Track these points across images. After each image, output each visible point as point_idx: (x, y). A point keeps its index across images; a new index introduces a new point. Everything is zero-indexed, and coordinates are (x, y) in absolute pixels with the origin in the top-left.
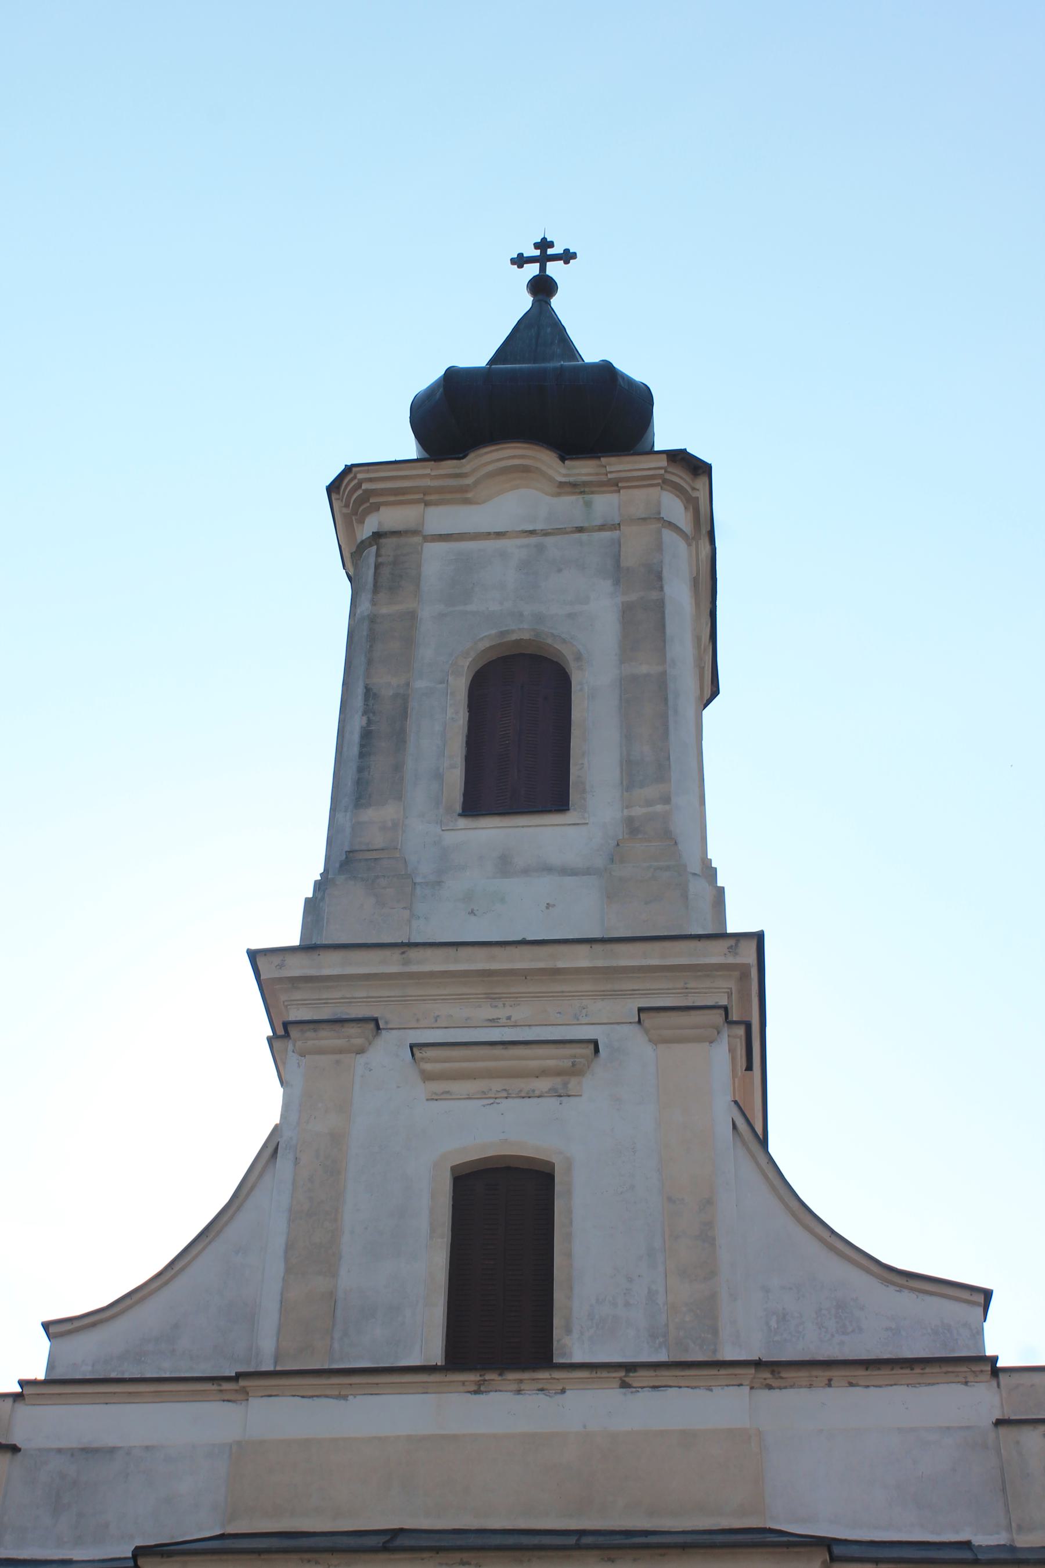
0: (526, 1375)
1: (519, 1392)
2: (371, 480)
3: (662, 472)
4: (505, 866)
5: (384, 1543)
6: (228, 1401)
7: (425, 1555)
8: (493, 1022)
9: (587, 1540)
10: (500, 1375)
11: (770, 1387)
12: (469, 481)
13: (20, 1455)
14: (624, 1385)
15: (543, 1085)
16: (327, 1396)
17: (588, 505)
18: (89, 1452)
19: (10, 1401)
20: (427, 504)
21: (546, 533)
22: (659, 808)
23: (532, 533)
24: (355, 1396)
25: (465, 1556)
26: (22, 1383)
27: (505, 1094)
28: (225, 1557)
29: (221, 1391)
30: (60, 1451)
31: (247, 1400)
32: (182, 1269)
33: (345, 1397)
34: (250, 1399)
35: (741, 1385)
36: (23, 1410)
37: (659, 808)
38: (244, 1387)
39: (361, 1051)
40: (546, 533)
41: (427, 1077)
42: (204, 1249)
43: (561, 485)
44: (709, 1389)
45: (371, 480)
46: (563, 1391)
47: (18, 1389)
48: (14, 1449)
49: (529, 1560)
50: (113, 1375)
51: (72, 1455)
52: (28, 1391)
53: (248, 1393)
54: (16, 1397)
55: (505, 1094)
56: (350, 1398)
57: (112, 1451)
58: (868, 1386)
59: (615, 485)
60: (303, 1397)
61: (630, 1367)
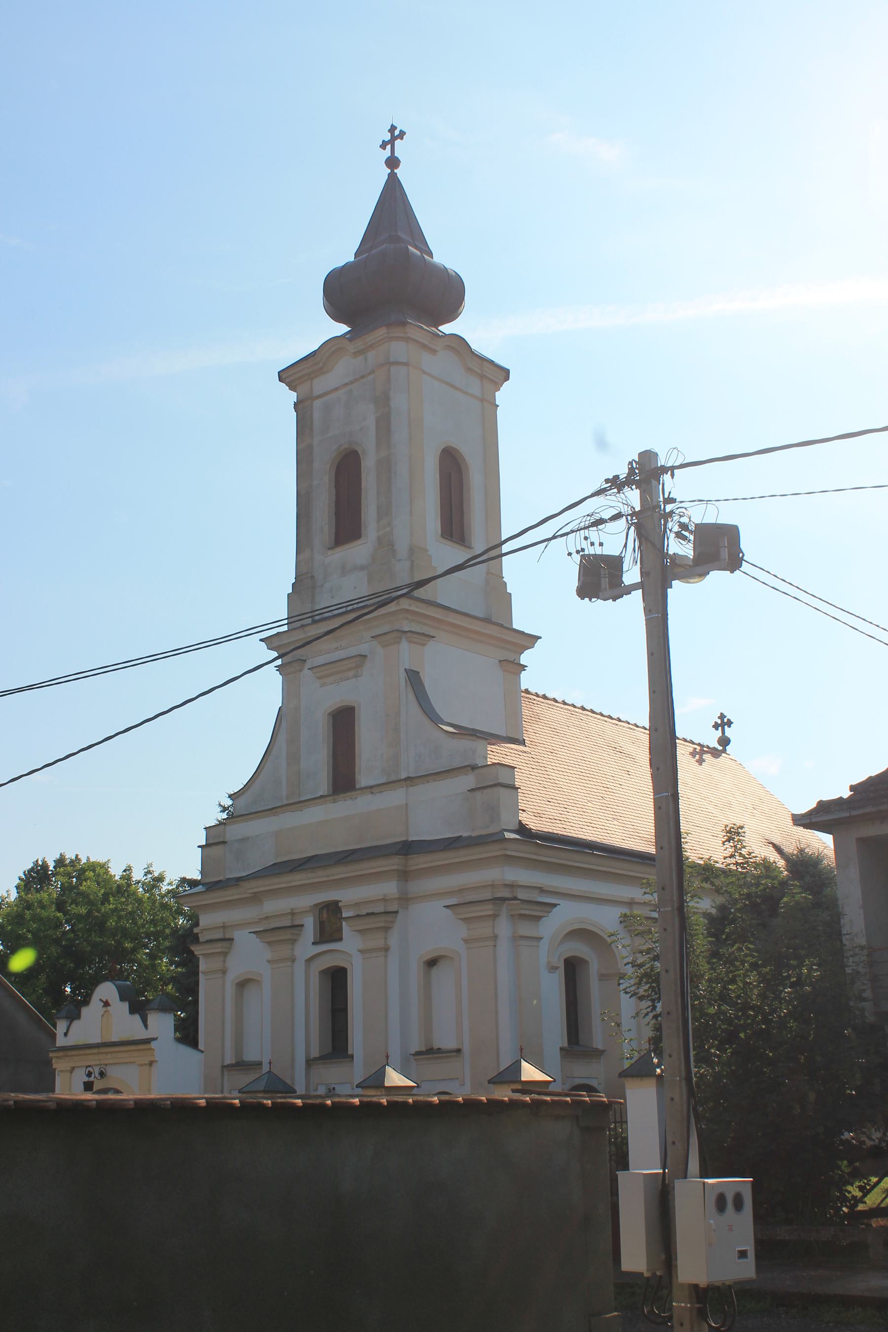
0: (345, 795)
1: (345, 800)
2: (288, 377)
3: (386, 335)
4: (344, 570)
8: (337, 649)
10: (338, 796)
11: (413, 786)
12: (321, 365)
14: (372, 793)
15: (351, 673)
17: (366, 359)
20: (312, 379)
21: (351, 383)
22: (388, 529)
23: (346, 384)
27: (341, 680)
30: (236, 841)
32: (263, 768)
33: (302, 810)
35: (403, 787)
37: (388, 529)
39: (301, 670)
40: (351, 383)
41: (319, 678)
42: (267, 760)
43: (354, 353)
44: (395, 790)
45: (288, 377)
46: (356, 798)
48: (224, 842)
55: (341, 680)
58: (439, 781)
59: (372, 347)
61: (371, 787)
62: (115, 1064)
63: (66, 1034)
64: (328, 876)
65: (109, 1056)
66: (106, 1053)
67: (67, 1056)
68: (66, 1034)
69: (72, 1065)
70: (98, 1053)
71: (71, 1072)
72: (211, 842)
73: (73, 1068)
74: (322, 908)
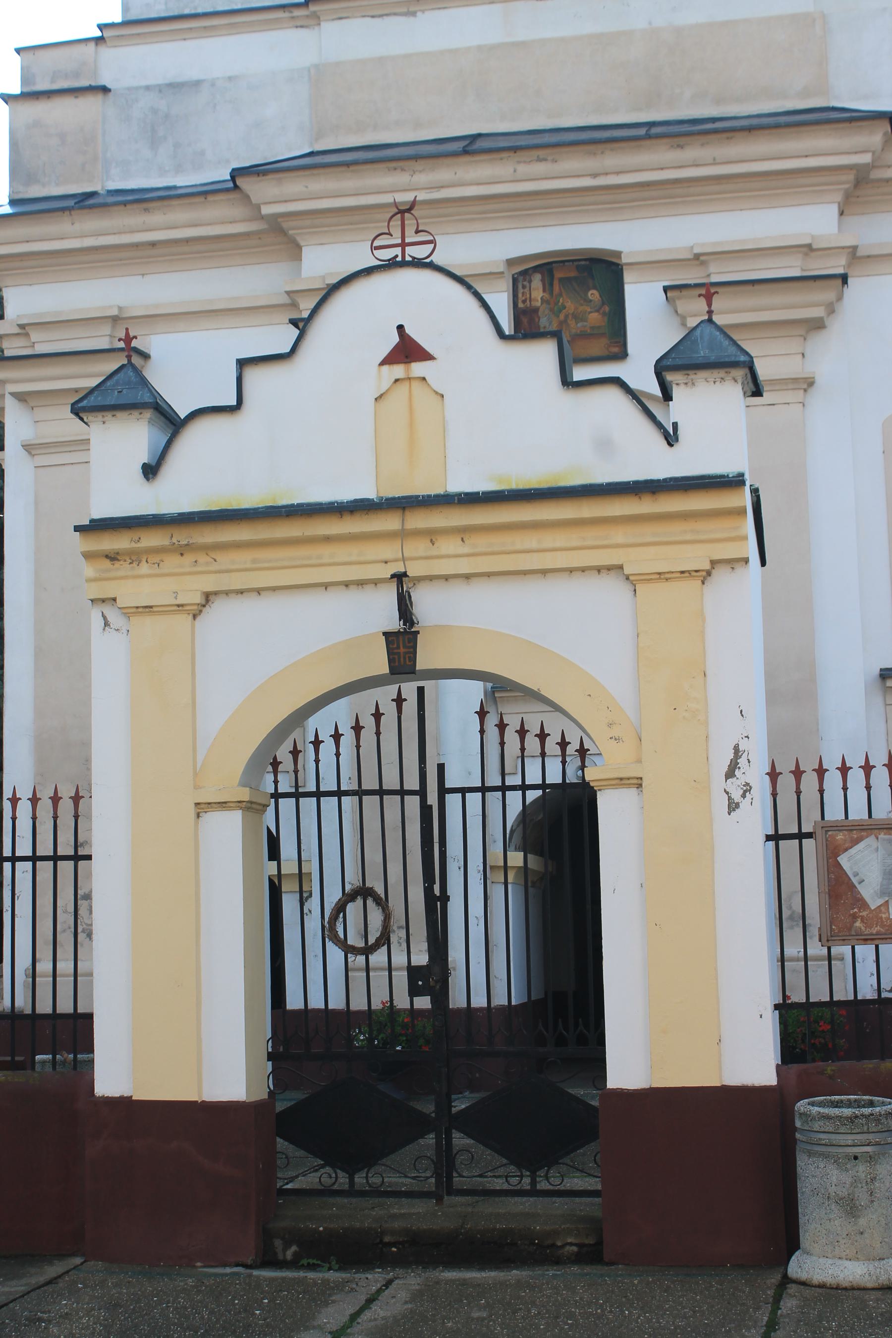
5: (464, 147)
6: (302, 27)
7: (504, 155)
9: (655, 130)
13: (111, 95)
16: (395, 14)
18: (175, 87)
19: (92, 45)
24: (423, 11)
25: (541, 153)
26: (101, 27)
28: (315, 172)
29: (293, 18)
30: (148, 88)
31: (319, 24)
33: (414, 14)
34: (322, 24)
36: (107, 53)
38: (315, 12)
47: (99, 34)
48: (105, 90)
49: (602, 153)
50: (187, 11)
51: (160, 91)
52: (107, 34)
53: (319, 18)
54: (99, 40)
56: (419, 14)
57: (197, 84)
60: (373, 17)
62: (467, 577)
63: (150, 471)
64: (595, 176)
65: (448, 546)
66: (431, 535)
67: (181, 550)
68: (150, 471)
69: (209, 583)
70: (403, 535)
71: (195, 617)
72: (42, 85)
73: (208, 597)
74: (525, 274)
